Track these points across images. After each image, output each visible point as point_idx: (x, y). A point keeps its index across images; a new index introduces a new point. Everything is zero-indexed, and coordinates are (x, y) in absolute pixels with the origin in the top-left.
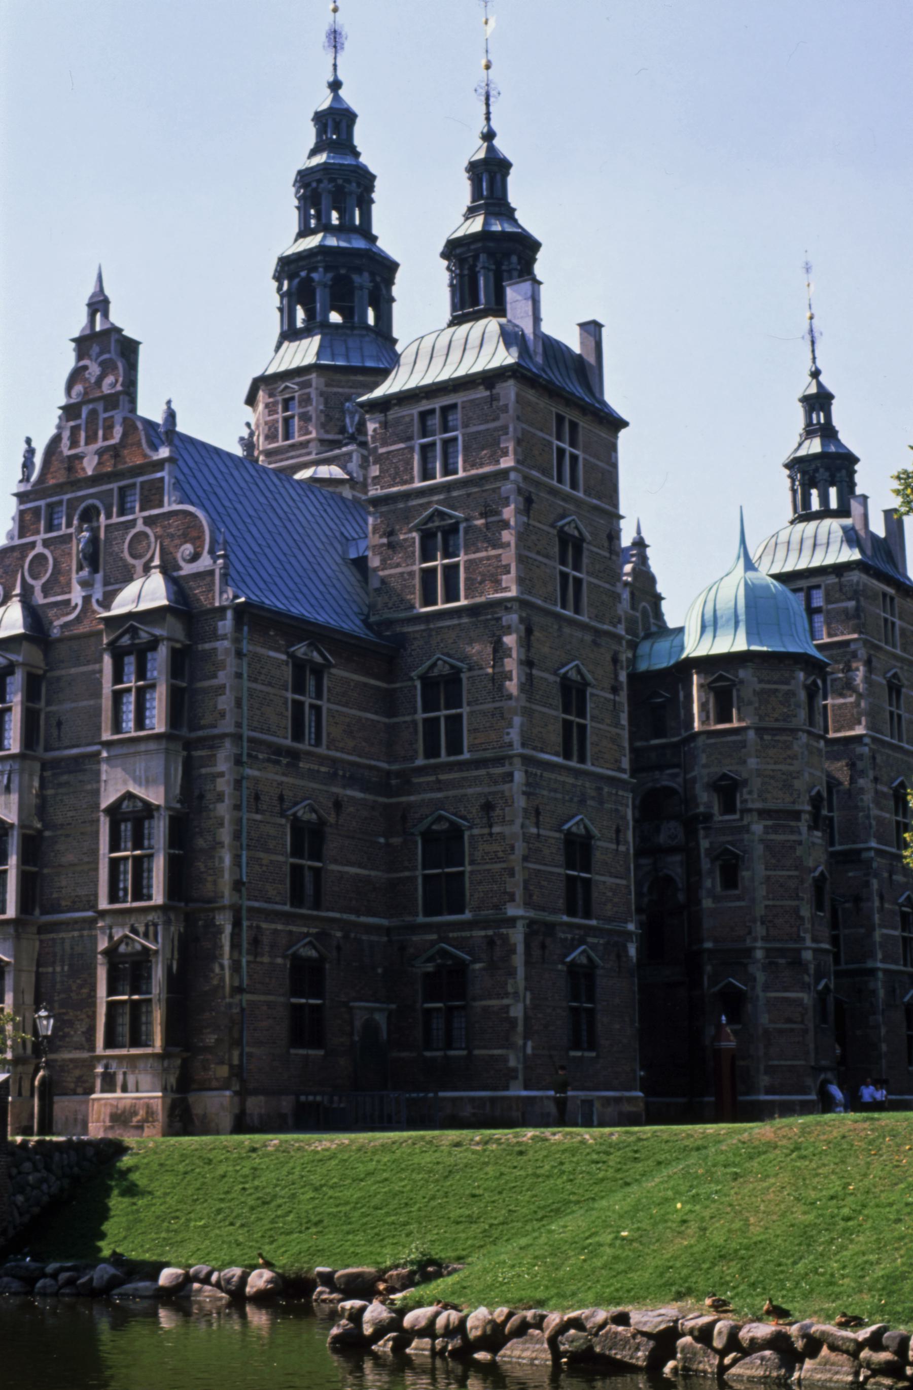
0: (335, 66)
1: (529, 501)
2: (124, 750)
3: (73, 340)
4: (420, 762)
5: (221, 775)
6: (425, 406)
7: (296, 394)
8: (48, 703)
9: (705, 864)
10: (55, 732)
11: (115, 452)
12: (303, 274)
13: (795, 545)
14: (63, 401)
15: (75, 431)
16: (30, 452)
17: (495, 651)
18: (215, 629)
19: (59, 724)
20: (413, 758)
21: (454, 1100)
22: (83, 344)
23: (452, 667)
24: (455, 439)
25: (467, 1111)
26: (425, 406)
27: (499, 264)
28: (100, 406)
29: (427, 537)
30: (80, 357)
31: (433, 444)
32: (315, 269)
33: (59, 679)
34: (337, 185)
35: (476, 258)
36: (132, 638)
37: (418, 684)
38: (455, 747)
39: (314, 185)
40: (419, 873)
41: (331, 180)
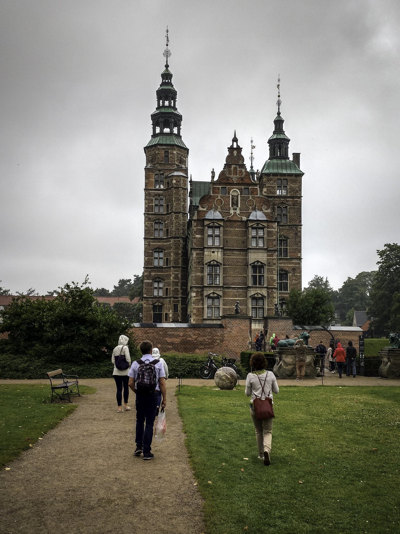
5: (275, 259)
6: (279, 177)
7: (169, 151)
10: (226, 243)
11: (242, 179)
12: (166, 118)
14: (225, 163)
16: (213, 173)
18: (273, 227)
19: (227, 242)
22: (231, 149)
26: (279, 177)
28: (238, 167)
29: (278, 207)
32: (170, 117)
33: (227, 230)
34: (166, 93)
35: (282, 144)
36: (258, 225)
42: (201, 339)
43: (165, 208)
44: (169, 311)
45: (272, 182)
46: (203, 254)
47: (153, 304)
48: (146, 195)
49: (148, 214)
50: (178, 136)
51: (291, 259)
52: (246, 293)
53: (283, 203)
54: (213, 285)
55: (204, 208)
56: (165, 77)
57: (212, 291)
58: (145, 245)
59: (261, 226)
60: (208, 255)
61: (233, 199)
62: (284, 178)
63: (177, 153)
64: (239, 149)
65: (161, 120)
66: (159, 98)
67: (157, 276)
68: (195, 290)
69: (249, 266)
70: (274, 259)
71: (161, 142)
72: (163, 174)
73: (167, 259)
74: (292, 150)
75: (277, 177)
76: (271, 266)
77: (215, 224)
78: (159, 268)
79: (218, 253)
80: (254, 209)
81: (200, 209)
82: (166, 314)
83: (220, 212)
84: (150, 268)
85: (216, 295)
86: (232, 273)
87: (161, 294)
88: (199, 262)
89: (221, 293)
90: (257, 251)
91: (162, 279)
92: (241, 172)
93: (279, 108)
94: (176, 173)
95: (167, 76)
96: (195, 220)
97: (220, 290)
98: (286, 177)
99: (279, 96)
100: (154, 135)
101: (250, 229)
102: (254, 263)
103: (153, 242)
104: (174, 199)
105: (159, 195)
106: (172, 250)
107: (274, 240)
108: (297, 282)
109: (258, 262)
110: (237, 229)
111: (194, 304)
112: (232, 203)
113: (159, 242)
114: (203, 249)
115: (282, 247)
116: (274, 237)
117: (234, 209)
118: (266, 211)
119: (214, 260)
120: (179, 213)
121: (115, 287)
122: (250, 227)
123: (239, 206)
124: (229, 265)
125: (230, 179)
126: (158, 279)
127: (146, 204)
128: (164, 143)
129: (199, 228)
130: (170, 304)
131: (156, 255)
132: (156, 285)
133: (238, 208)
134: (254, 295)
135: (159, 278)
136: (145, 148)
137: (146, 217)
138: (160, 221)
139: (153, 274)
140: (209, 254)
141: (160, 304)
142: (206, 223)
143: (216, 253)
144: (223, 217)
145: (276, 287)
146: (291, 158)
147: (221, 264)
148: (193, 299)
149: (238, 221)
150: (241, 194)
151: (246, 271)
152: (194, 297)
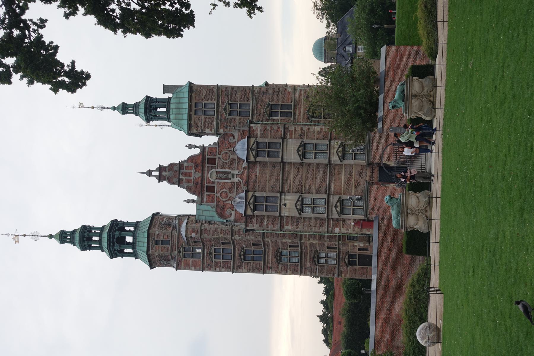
0: (44, 236)
2: (285, 153)
3: (159, 182)
4: (292, 119)
5: (295, 128)
6: (193, 113)
7: (156, 239)
11: (197, 166)
12: (115, 240)
14: (177, 186)
15: (187, 181)
16: (188, 201)
18: (255, 130)
19: (273, 187)
20: (291, 121)
22: (160, 178)
23: (268, 107)
26: (193, 113)
28: (182, 171)
29: (230, 114)
30: (165, 180)
32: (114, 236)
33: (259, 187)
34: (84, 238)
35: (151, 106)
36: (253, 150)
37: (271, 118)
39: (85, 239)
40: (322, 119)
41: (85, 232)
42: (391, 245)
43: (226, 247)
44: (356, 246)
45: (198, 122)
46: (287, 217)
47: (347, 265)
48: (210, 270)
49: (234, 268)
50: (136, 225)
51: (295, 100)
52: (336, 165)
53: (225, 109)
54: (326, 206)
55: (231, 214)
56: (65, 239)
57: (334, 208)
58: (272, 273)
59: (255, 145)
60: (289, 212)
61: (221, 178)
62: (193, 106)
63: (158, 229)
64: (161, 169)
65: (116, 248)
66: (90, 248)
67: (312, 259)
68: (331, 229)
69: (303, 162)
70: (295, 129)
71: (145, 249)
72: (184, 248)
73: (290, 246)
74: (158, 94)
75: (193, 115)
76: (304, 134)
77: (251, 201)
78: (302, 255)
79: (287, 200)
80: (234, 152)
81: (232, 218)
82: (359, 249)
83: (236, 195)
84: (301, 267)
85: (338, 204)
86: (311, 182)
87: (334, 255)
88: (298, 222)
89: (336, 198)
90: (285, 151)
91: (315, 254)
92: (188, 168)
93: (107, 108)
94: (183, 233)
95: (63, 237)
96: (246, 226)
97: (333, 198)
98: (193, 104)
99: (93, 108)
100: (135, 255)
102: (300, 155)
103: (269, 263)
104: (215, 236)
105: (210, 253)
106: (279, 241)
107: (272, 129)
109: (298, 150)
110: (258, 174)
111: (348, 229)
112: (226, 179)
113: (268, 256)
114: (282, 218)
115: (280, 111)
116: (268, 128)
117: (233, 177)
118: (236, 137)
119: (296, 205)
120: (232, 230)
121: (322, 302)
122: (255, 159)
123: (229, 170)
124: (302, 186)
126: (316, 258)
127: (220, 271)
128: (146, 245)
129: (255, 221)
130: (347, 245)
131: (285, 259)
132: (323, 261)
133: (232, 172)
134: (339, 156)
135: (314, 257)
136: (151, 268)
137: (237, 271)
138: (242, 253)
139: (308, 264)
140: (288, 210)
141: (347, 257)
142: (249, 212)
143: (287, 202)
144: (242, 191)
146: (170, 95)
147: (300, 196)
148: (343, 230)
149: (248, 172)
150: (215, 168)
151: (309, 164)
152: (340, 229)
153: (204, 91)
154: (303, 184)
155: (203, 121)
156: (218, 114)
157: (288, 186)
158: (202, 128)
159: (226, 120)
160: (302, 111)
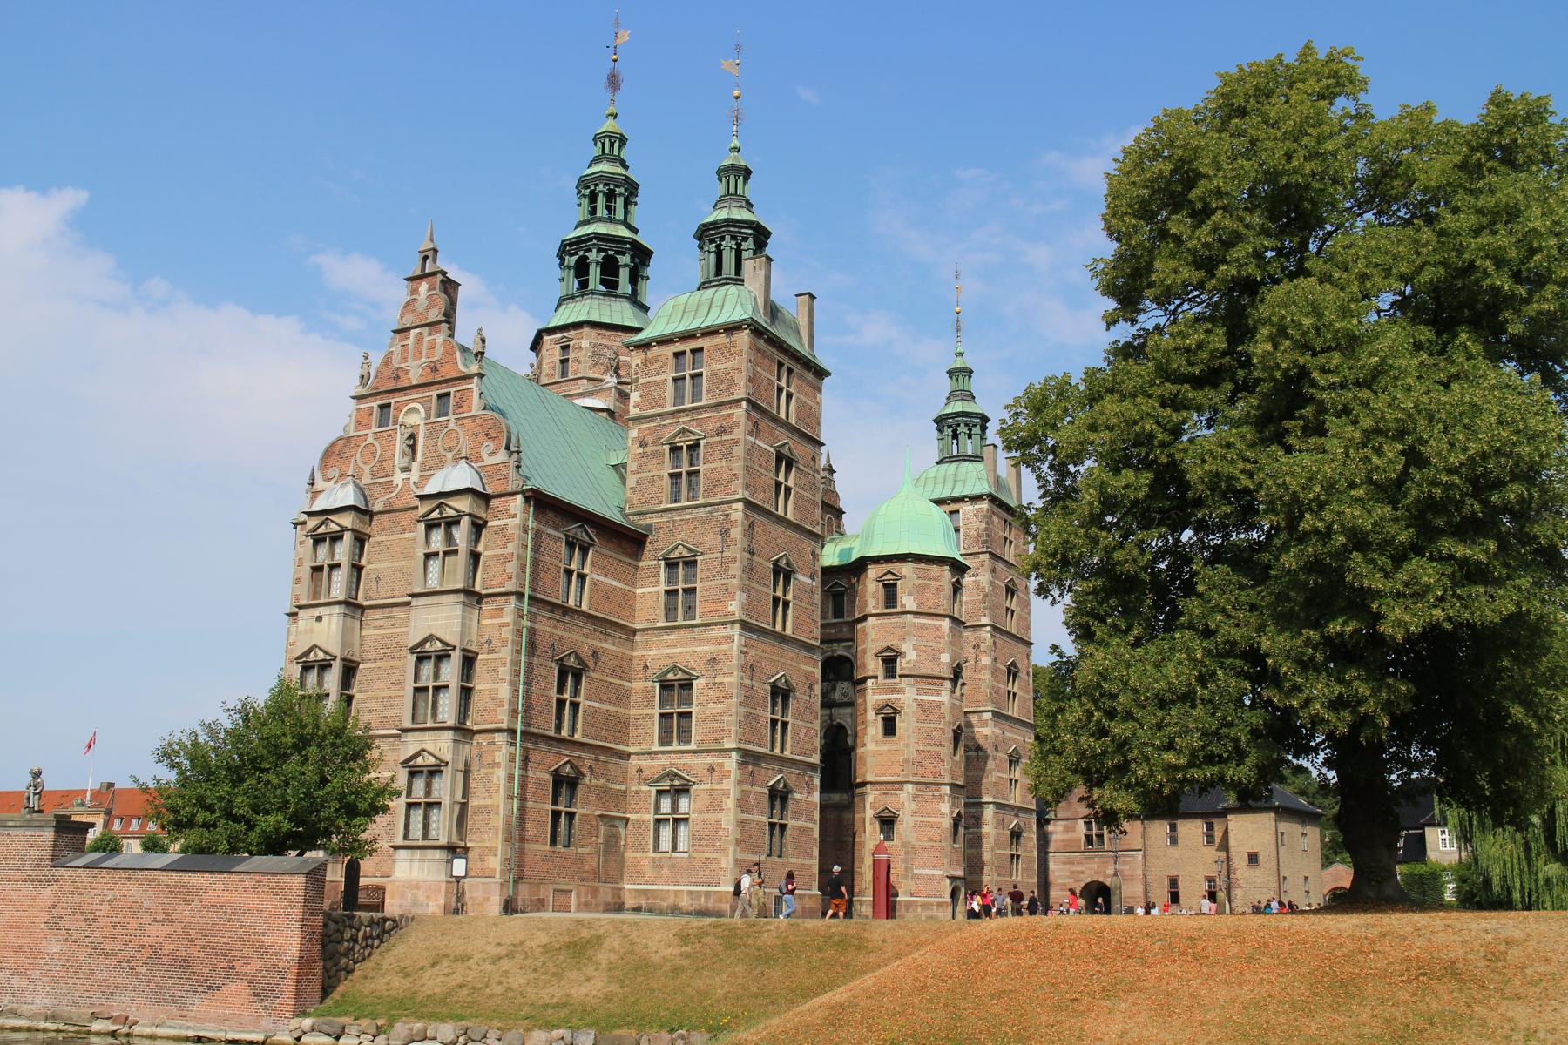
1: (756, 424)
6: (678, 347)
8: (369, 562)
9: (871, 715)
13: (940, 480)
17: (724, 540)
19: (378, 580)
21: (676, 893)
23: (690, 550)
24: (701, 375)
25: (685, 903)
26: (678, 347)
27: (739, 245)
29: (675, 449)
31: (683, 378)
35: (722, 239)
38: (690, 610)
45: (657, 365)
53: (684, 431)
76: (491, 651)
80: (456, 460)
101: (422, 526)
108: (720, 708)
109: (430, 638)
110: (407, 535)
115: (680, 586)
125: (402, 375)
133: (415, 466)
143: (325, 620)
145: (504, 725)
150: (428, 417)
153: (729, 365)
154: (379, 664)
155: (657, 378)
156: (673, 413)
157: (376, 623)
158: (642, 381)
159: (658, 441)
160: (678, 650)
